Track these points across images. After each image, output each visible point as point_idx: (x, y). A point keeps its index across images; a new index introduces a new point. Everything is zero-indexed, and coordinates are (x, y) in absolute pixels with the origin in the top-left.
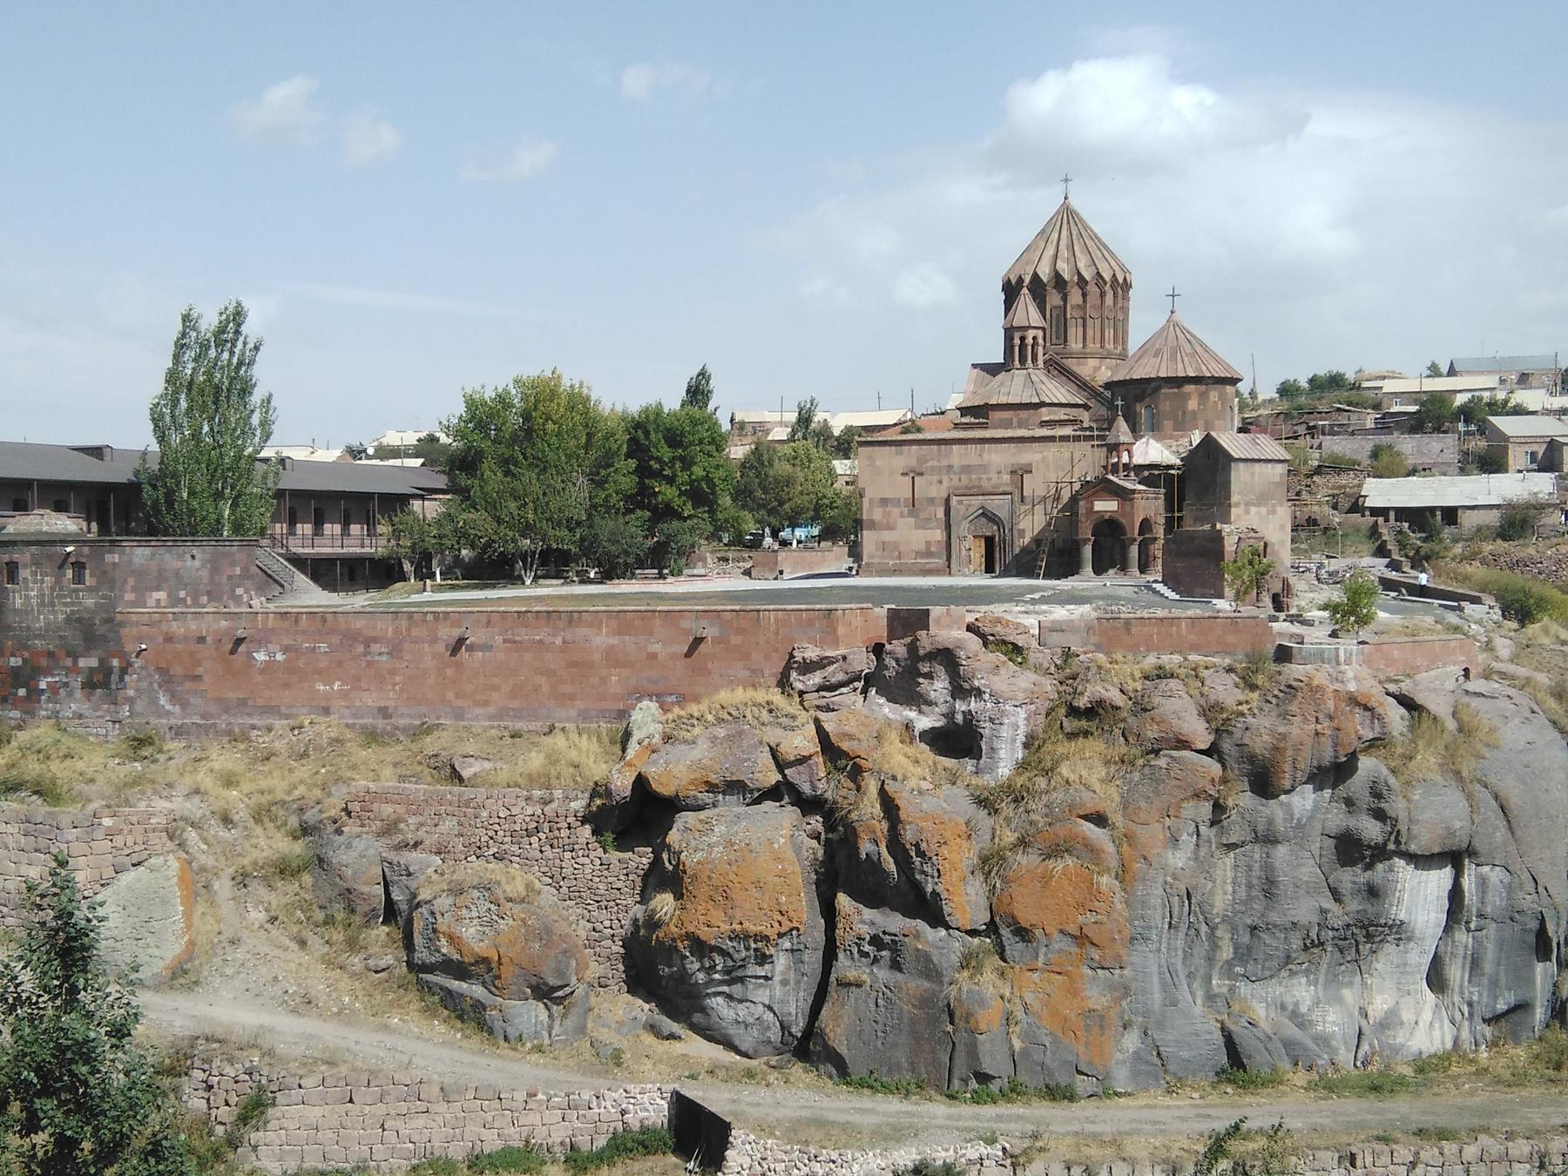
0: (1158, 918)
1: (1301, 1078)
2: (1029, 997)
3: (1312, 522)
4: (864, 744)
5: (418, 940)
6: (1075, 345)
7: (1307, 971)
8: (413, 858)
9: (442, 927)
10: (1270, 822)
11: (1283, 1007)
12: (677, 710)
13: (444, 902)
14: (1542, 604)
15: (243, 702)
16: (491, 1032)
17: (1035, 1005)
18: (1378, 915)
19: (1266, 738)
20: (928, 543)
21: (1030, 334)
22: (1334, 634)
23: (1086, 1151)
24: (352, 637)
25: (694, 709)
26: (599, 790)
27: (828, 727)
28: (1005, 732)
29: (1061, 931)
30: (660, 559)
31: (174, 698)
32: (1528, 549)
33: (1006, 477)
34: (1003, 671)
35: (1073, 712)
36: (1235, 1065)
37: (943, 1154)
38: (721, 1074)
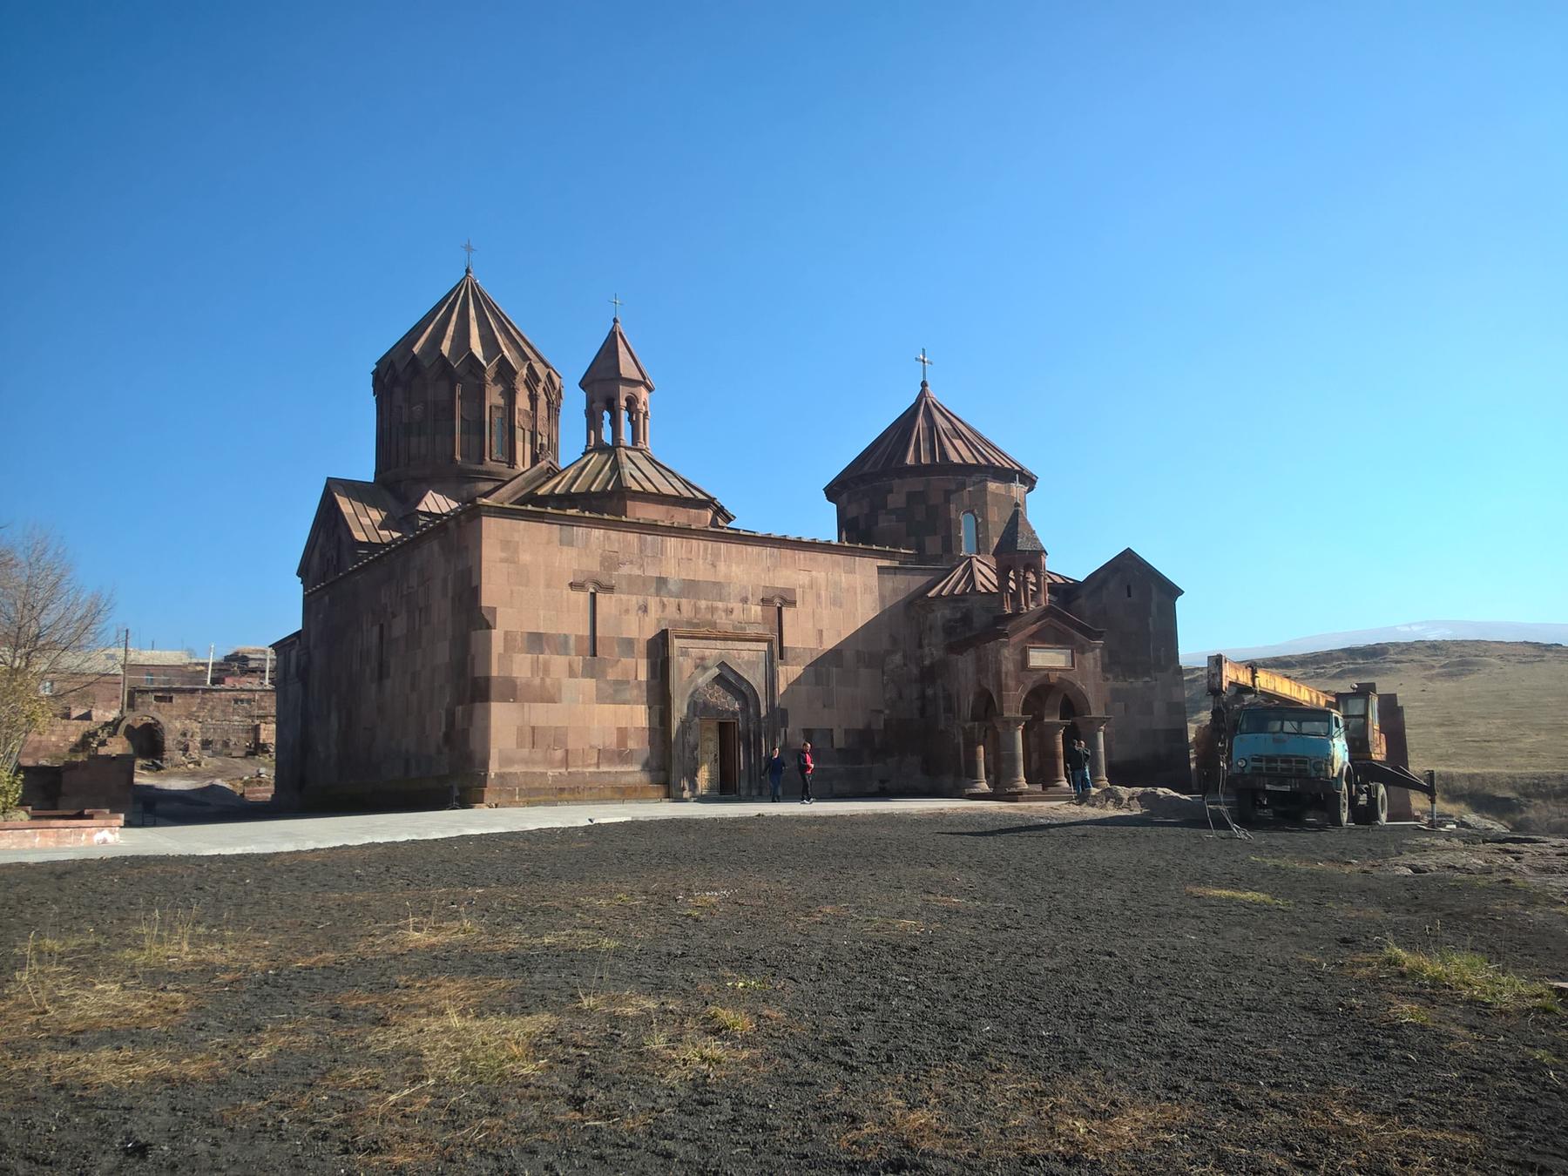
20: (623, 733)
33: (756, 610)
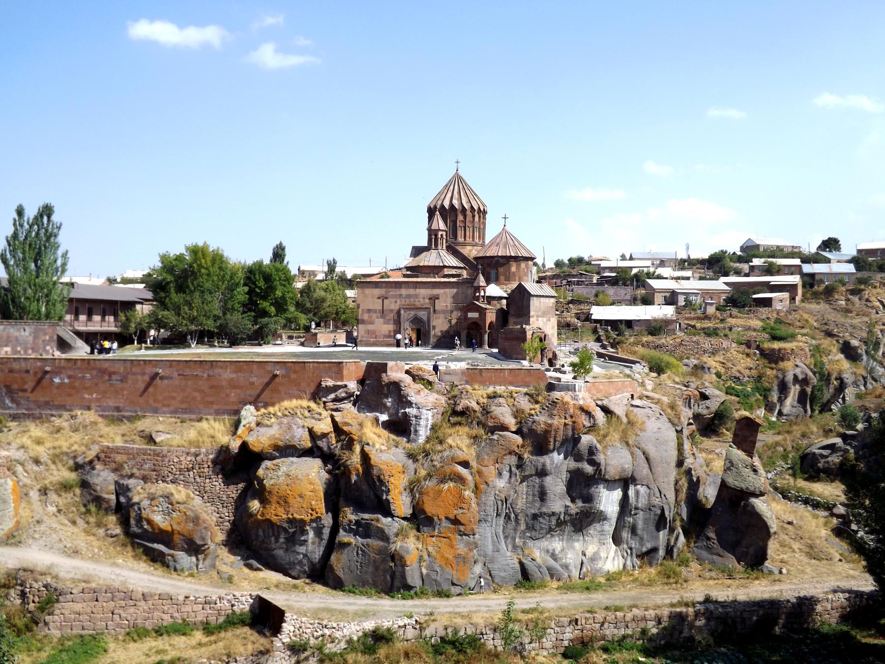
0: (492, 511)
1: (555, 584)
2: (430, 549)
3: (568, 325)
4: (354, 428)
5: (132, 522)
6: (460, 239)
7: (559, 535)
8: (131, 482)
9: (144, 516)
10: (544, 465)
11: (548, 551)
12: (263, 410)
13: (145, 503)
14: (668, 365)
15: (47, 403)
16: (168, 566)
17: (434, 553)
18: (591, 508)
19: (542, 426)
20: (390, 331)
21: (440, 233)
22: (575, 378)
23: (455, 620)
24: (103, 371)
25: (271, 409)
26: (224, 450)
27: (337, 419)
28: (423, 422)
29: (447, 518)
30: (259, 337)
31: (13, 400)
32: (663, 340)
33: (427, 301)
34: (422, 393)
35: (455, 413)
36: (525, 578)
37: (387, 623)
38: (282, 586)
